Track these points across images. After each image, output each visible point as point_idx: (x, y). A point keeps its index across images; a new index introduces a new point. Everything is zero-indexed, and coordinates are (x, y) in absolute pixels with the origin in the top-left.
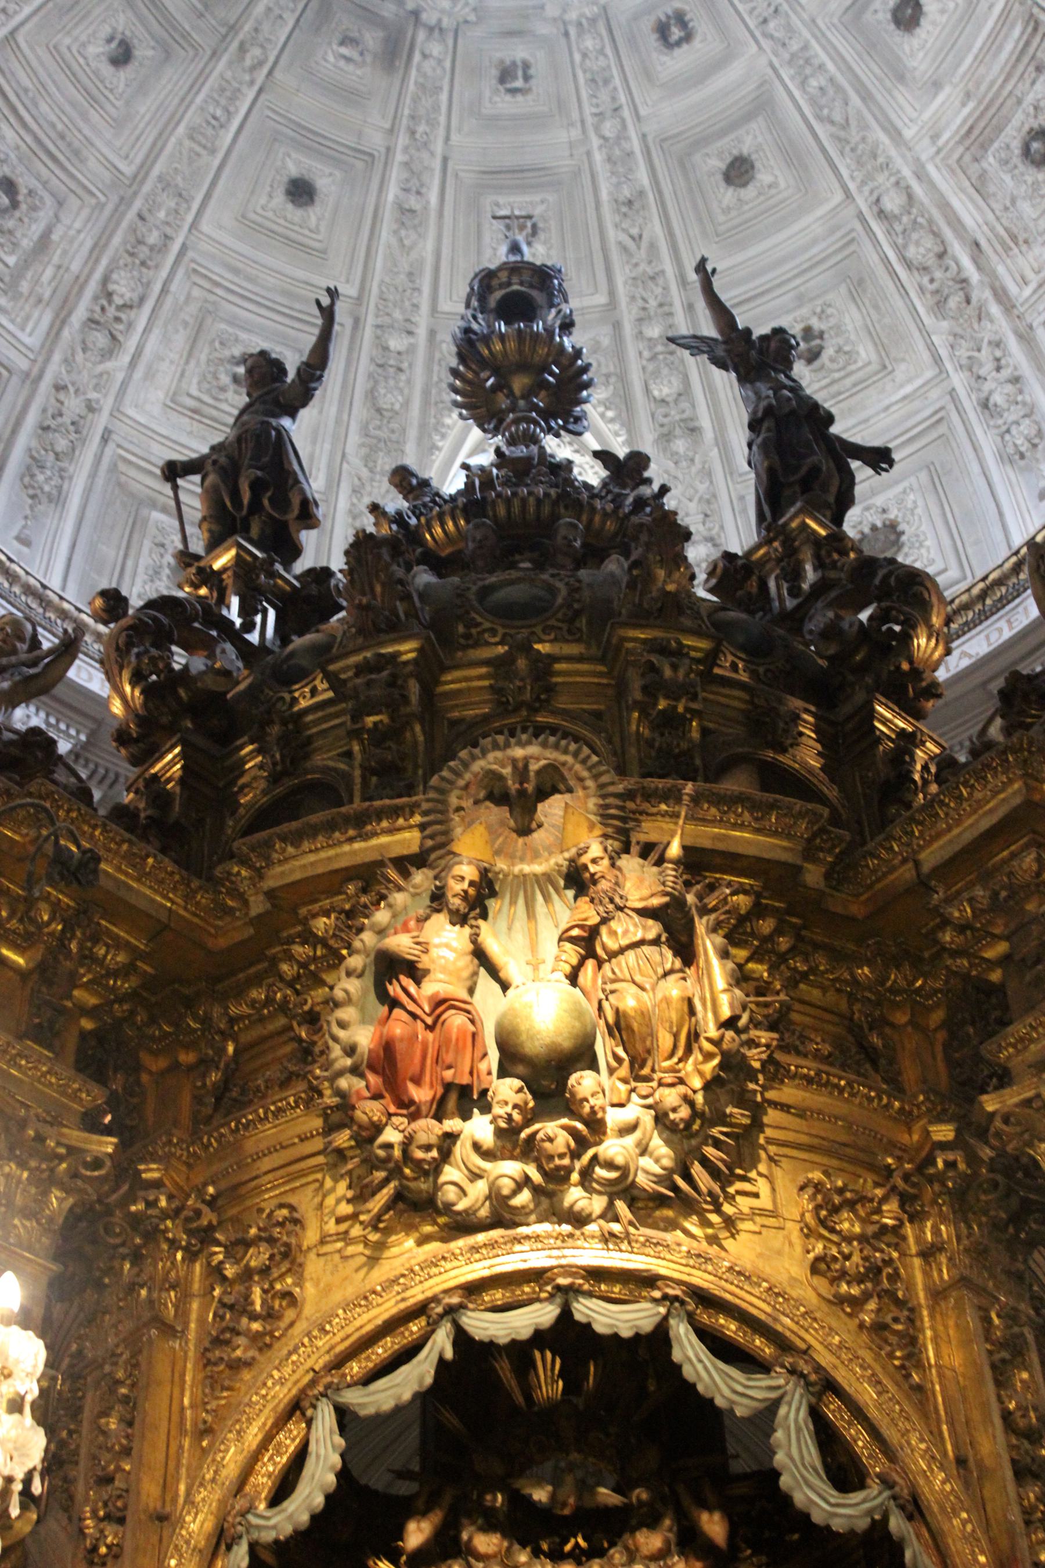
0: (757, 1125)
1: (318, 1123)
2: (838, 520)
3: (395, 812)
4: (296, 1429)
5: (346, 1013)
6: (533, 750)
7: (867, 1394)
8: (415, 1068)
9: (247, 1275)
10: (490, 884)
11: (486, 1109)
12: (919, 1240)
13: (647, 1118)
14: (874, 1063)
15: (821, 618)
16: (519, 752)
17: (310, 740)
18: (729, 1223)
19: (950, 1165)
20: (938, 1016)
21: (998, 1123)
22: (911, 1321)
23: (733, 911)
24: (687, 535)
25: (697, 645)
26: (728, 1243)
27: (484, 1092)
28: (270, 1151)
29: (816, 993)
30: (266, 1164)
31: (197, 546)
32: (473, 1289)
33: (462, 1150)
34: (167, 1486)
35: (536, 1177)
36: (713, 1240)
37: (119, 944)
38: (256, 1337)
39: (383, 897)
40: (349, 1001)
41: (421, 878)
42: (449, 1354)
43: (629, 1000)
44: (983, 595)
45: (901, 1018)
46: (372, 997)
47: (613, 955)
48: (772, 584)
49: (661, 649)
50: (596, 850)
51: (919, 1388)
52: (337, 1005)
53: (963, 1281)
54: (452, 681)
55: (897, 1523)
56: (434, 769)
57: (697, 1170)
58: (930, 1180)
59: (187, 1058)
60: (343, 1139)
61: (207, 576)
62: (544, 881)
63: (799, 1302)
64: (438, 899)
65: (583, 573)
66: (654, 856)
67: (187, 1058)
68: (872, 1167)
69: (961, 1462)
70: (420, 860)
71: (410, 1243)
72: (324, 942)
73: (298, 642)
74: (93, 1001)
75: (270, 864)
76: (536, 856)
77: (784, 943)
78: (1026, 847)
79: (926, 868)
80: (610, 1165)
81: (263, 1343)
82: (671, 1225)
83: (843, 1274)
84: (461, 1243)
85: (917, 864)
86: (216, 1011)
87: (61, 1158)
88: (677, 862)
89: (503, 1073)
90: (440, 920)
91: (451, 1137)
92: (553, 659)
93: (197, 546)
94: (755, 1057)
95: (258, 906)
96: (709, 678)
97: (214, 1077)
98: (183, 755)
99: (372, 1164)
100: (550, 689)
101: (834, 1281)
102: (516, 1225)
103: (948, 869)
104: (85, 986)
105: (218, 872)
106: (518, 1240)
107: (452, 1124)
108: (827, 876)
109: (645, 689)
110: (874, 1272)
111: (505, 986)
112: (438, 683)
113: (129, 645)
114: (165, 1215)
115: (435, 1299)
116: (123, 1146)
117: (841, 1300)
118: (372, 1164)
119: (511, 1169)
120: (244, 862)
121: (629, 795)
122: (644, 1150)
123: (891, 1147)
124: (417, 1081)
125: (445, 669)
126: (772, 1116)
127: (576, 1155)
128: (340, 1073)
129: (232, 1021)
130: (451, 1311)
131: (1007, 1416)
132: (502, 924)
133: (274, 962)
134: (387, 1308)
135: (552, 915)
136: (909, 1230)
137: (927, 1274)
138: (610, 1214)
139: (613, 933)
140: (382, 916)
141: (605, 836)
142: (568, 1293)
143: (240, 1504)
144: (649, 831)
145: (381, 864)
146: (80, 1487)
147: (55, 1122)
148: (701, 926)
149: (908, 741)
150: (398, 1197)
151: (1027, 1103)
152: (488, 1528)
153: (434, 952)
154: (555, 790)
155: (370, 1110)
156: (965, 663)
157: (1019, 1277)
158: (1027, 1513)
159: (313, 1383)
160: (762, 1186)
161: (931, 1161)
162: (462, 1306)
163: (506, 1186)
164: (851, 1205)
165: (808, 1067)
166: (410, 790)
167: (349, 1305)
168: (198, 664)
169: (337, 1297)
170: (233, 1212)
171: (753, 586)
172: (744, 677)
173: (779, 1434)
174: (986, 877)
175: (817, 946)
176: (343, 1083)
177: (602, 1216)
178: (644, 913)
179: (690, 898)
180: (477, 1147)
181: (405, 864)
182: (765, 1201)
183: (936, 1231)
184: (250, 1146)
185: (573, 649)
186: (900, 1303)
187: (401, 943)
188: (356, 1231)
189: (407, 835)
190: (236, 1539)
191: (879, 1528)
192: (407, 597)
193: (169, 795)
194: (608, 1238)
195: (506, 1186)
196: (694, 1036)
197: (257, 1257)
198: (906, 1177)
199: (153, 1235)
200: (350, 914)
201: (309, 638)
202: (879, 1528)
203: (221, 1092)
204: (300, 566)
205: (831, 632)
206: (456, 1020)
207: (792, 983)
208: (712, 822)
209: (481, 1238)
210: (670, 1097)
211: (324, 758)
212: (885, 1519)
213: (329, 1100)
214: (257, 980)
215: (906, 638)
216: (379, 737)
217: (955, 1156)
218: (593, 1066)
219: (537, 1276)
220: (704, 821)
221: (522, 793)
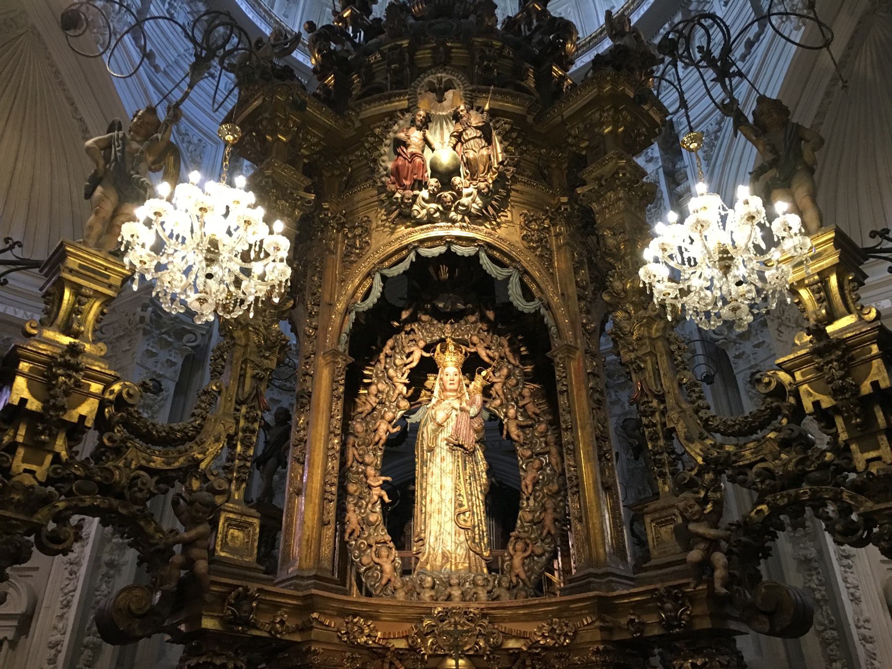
0: (508, 196)
1: (376, 192)
2: (545, 6)
3: (400, 95)
4: (369, 281)
5: (385, 158)
6: (444, 75)
7: (537, 274)
9: (355, 237)
10: (429, 118)
11: (426, 188)
12: (555, 231)
13: (475, 192)
14: (545, 180)
15: (537, 37)
16: (439, 75)
17: (374, 73)
18: (499, 224)
19: (566, 209)
20: (565, 165)
21: (581, 196)
22: (551, 254)
23: (504, 129)
24: (496, 7)
25: (496, 44)
26: (498, 230)
27: (426, 183)
28: (362, 200)
29: (528, 157)
30: (360, 204)
31: (338, 9)
32: (422, 241)
33: (419, 200)
34: (332, 296)
35: (441, 208)
36: (493, 229)
37: (315, 136)
38: (357, 254)
39: (396, 122)
40: (385, 154)
42: (414, 260)
43: (471, 155)
44: (589, 42)
45: (554, 166)
46: (393, 153)
47: (467, 141)
48: (522, 27)
49: (486, 44)
50: (462, 107)
51: (552, 274)
52: (382, 155)
53: (567, 244)
54: (419, 55)
55: (543, 311)
56: (413, 80)
57: (489, 208)
58: (559, 214)
59: (337, 172)
60: (383, 196)
61: (341, 19)
62: (446, 118)
63: (518, 247)
65: (462, 20)
66: (480, 110)
67: (337, 172)
68: (542, 210)
69: (563, 295)
70: (408, 110)
71: (403, 228)
72: (378, 136)
73: (370, 42)
74: (307, 153)
75: (361, 111)
76: (443, 110)
77: (519, 141)
78: (597, 111)
79: (565, 117)
80: (463, 205)
81: (359, 256)
82: (481, 225)
83: (532, 240)
85: (562, 116)
86: (345, 158)
87: (298, 200)
88: (488, 111)
89: (432, 177)
90: (414, 129)
91: (416, 196)
92: (452, 48)
93: (338, 9)
95: (358, 124)
96: (501, 55)
97: (345, 178)
98: (334, 78)
99: (392, 204)
100: (450, 58)
101: (529, 242)
102: (434, 223)
103: (572, 117)
104: (305, 148)
105: (345, 113)
106: (435, 227)
107: (416, 192)
108: (534, 119)
109: (480, 58)
110: (541, 240)
111: (433, 150)
112: (414, 55)
113: (317, 40)
114: (330, 219)
115: (410, 244)
116: (317, 198)
117: (530, 248)
118: (392, 204)
119: (434, 206)
120: (353, 110)
121: (473, 91)
122: (474, 201)
123: (548, 204)
124: (406, 179)
125: (417, 50)
126: (513, 193)
127: (453, 202)
128: (383, 176)
129: (350, 161)
130: (415, 248)
131: (577, 282)
132: (433, 131)
134: (396, 246)
135: (448, 128)
136: (552, 228)
137: (556, 241)
138: (463, 220)
139: (467, 134)
140: (396, 128)
141: (465, 103)
142: (449, 244)
143: (353, 301)
144: (479, 103)
145: (396, 111)
146: (306, 297)
147: (296, 189)
148: (494, 133)
149: (563, 78)
150: (400, 214)
151: (590, 191)
152: (425, 314)
153: (412, 139)
154: (451, 88)
155: (392, 187)
156: (582, 64)
157: (583, 243)
158: (581, 309)
159: (374, 268)
160: (509, 214)
162: (418, 247)
163: (432, 211)
164: (535, 220)
165: (525, 179)
166: (406, 88)
167: (385, 245)
168: (339, 48)
169: (381, 243)
171: (516, 27)
172: (511, 56)
173: (510, 285)
176: (383, 179)
177: (461, 221)
178: (476, 128)
179: (491, 124)
180: (423, 199)
181: (403, 111)
182: (509, 218)
183: (560, 229)
184: (356, 199)
185: (458, 45)
186: (548, 249)
187: (402, 135)
188: (387, 224)
189: (404, 102)
191: (537, 312)
192: (405, 26)
193: (330, 91)
194: (462, 227)
195: (432, 211)
196: (490, 167)
197: (358, 231)
198: (552, 213)
199: (327, 224)
200: (386, 127)
201: (374, 40)
202: (537, 312)
203: (348, 182)
204: (371, 17)
205: (541, 42)
206: (418, 160)
207: (521, 154)
208: (500, 101)
209: (424, 226)
210: (482, 185)
211: (378, 79)
212: (539, 310)
213: (379, 184)
214: (357, 149)
215: (564, 44)
216: (396, 72)
217: (567, 207)
218: (460, 175)
219: (441, 238)
220: (496, 100)
221: (440, 88)
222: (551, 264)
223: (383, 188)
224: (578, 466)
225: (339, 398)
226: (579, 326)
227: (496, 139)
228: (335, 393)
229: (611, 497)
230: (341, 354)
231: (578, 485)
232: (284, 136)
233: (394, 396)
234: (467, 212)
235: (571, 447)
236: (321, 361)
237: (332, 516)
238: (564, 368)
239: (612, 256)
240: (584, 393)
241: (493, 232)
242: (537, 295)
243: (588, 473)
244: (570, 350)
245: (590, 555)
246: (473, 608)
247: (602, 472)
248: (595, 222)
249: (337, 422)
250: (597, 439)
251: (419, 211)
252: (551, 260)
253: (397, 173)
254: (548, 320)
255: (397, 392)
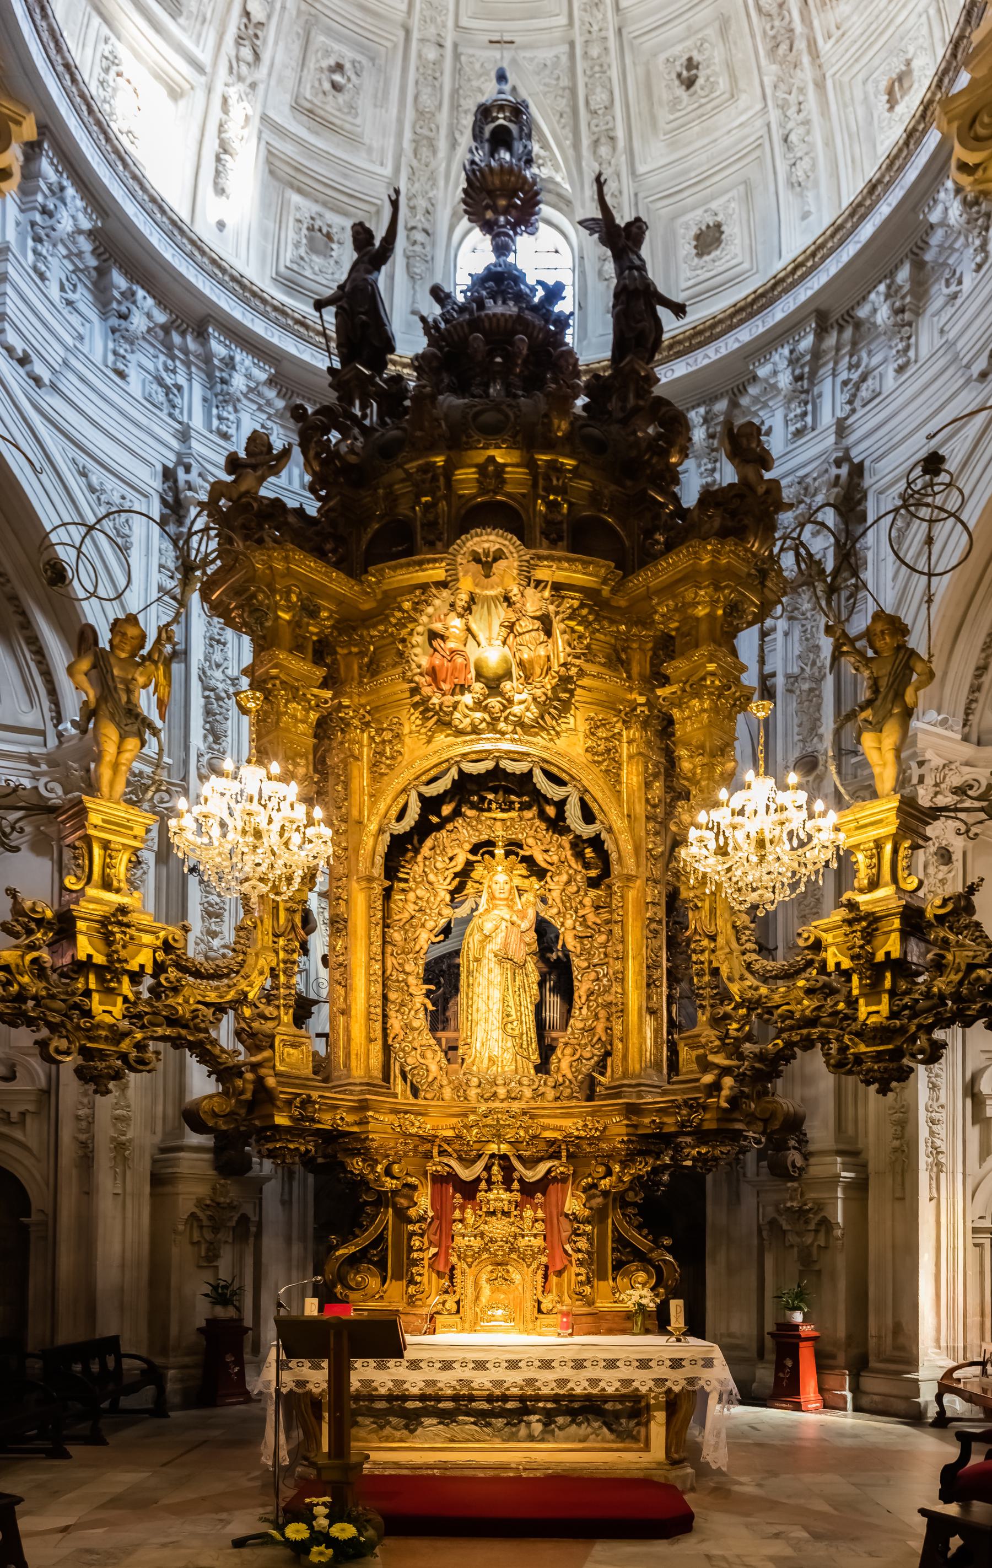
5: (417, 650)
7: (599, 795)
8: (443, 677)
11: (470, 692)
29: (602, 637)
35: (488, 719)
40: (418, 645)
41: (445, 593)
57: (547, 717)
60: (417, 698)
64: (452, 605)
76: (492, 587)
84: (460, 740)
89: (477, 680)
90: (453, 614)
94: (573, 671)
111: (479, 645)
117: (595, 762)
118: (427, 710)
123: (622, 701)
126: (579, 691)
132: (478, 616)
133: (387, 617)
143: (386, 821)
150: (438, 720)
153: (451, 630)
160: (572, 720)
161: (635, 709)
170: (377, 716)
174: (674, 597)
175: (605, 618)
176: (417, 678)
187: (437, 626)
190: (384, 832)
196: (549, 669)
200: (417, 603)
206: (459, 660)
209: (468, 738)
214: (381, 622)
218: (511, 679)
222: (619, 782)
223: (415, 691)
224: (624, 993)
225: (377, 924)
226: (643, 853)
227: (557, 627)
228: (373, 920)
229: (656, 1020)
230: (376, 879)
231: (623, 1011)
232: (286, 612)
233: (435, 902)
234: (520, 723)
235: (620, 976)
236: (355, 886)
237: (378, 1034)
238: (622, 897)
239: (687, 779)
240: (639, 924)
241: (550, 745)
242: (599, 816)
243: (634, 999)
244: (629, 878)
245: (627, 1069)
246: (516, 1106)
247: (649, 998)
248: (673, 734)
249: (377, 948)
250: (648, 967)
251: (461, 719)
252: (619, 775)
253: (433, 673)
254: (609, 845)
255: (439, 899)
